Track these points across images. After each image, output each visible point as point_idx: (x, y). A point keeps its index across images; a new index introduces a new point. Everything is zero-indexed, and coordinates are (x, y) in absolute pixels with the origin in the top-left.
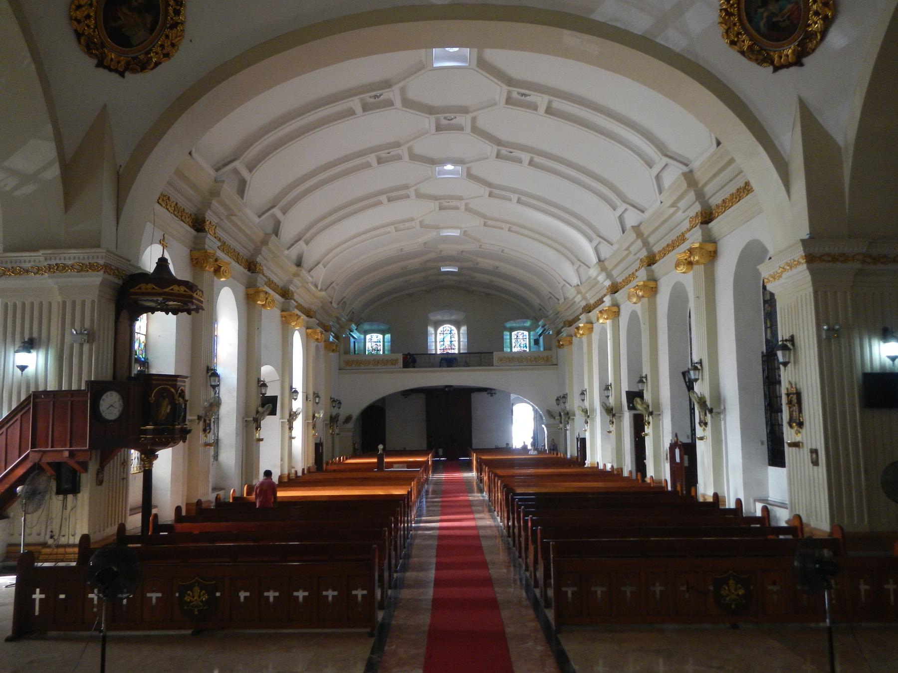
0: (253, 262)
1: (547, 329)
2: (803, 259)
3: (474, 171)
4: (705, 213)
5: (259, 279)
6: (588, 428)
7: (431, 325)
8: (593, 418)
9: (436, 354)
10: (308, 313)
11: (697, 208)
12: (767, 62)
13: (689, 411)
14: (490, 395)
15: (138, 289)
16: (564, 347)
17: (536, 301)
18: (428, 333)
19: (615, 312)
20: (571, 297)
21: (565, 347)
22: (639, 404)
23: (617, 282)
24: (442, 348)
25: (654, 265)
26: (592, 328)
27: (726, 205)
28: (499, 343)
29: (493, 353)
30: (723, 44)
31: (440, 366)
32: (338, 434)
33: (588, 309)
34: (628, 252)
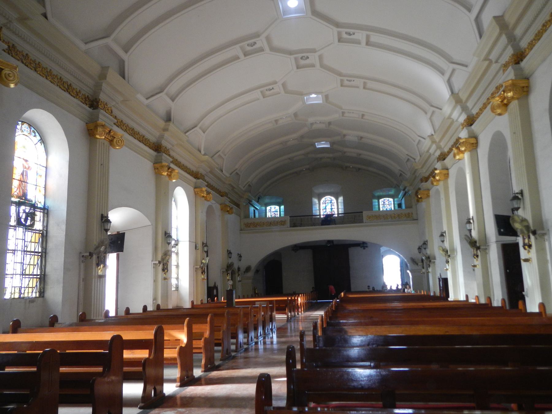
0: (96, 99)
1: (407, 192)
3: (320, 7)
5: (101, 116)
6: (449, 267)
7: (315, 197)
8: (454, 257)
10: (196, 175)
14: (363, 248)
16: (422, 201)
17: (395, 168)
18: (313, 203)
20: (426, 149)
21: (424, 200)
22: (517, 222)
23: (473, 114)
24: (325, 214)
25: (525, 60)
26: (448, 174)
29: (362, 212)
32: (240, 281)
34: (487, 63)
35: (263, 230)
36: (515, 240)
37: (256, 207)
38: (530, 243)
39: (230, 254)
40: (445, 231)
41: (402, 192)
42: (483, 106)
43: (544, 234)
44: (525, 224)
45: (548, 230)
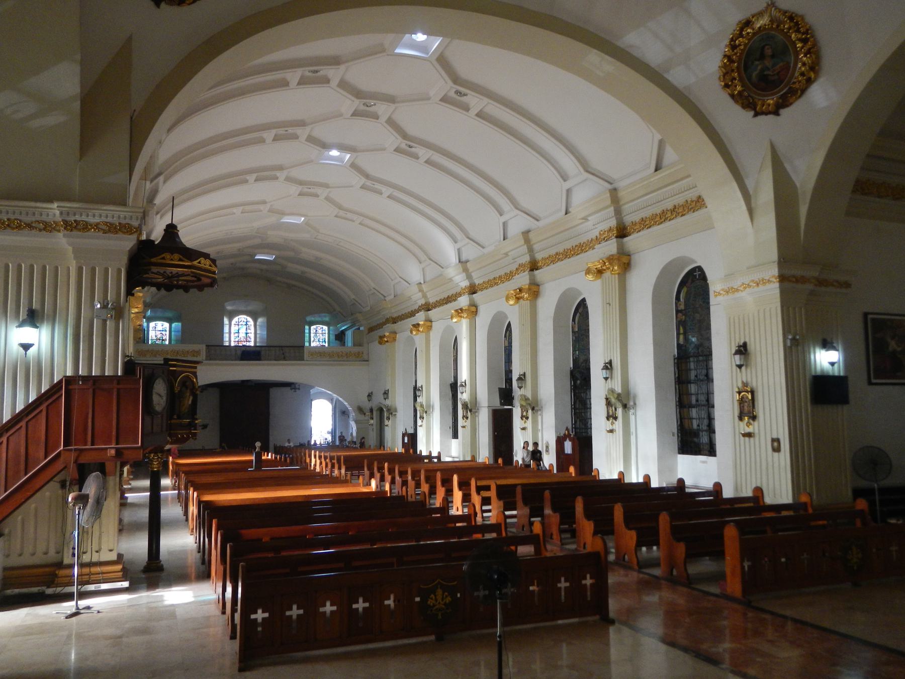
2: (776, 279)
4: (620, 228)
7: (227, 317)
8: (430, 414)
9: (230, 346)
11: (613, 223)
12: (751, 107)
13: (570, 407)
15: (161, 259)
16: (385, 344)
19: (473, 311)
24: (237, 340)
25: (537, 271)
26: (431, 326)
27: (645, 224)
30: (716, 85)
31: (242, 359)
33: (427, 307)
34: (504, 255)
42: (488, 282)
45: (542, 407)
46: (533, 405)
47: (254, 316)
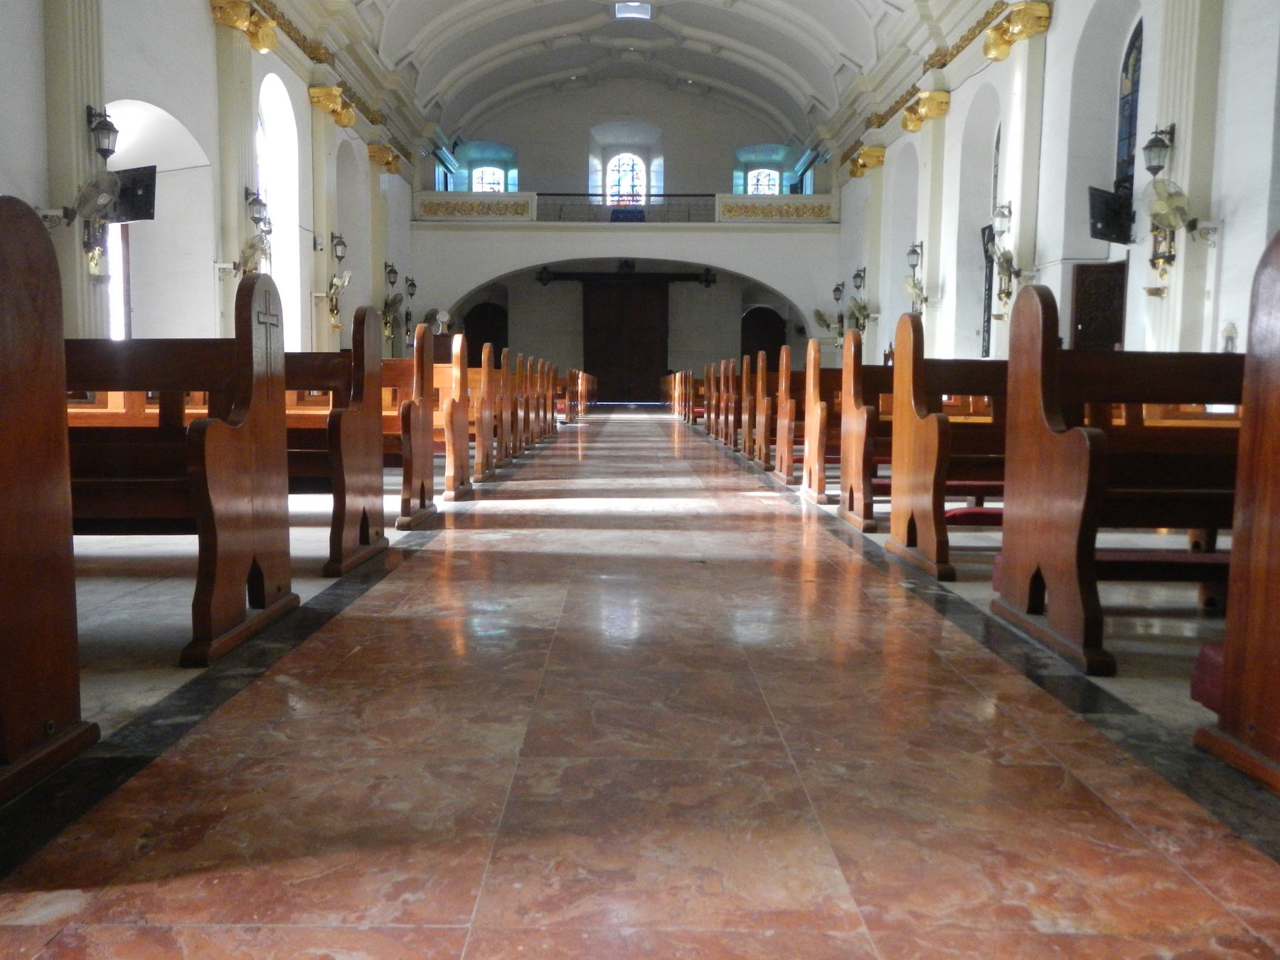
7: (596, 156)
8: (935, 303)
10: (315, 52)
14: (704, 284)
16: (862, 174)
17: (801, 89)
18: (591, 170)
21: (867, 172)
26: (947, 103)
28: (728, 186)
29: (714, 196)
35: (469, 223)
36: (1106, 257)
37: (449, 166)
38: (1173, 253)
39: (392, 275)
40: (922, 243)
41: (808, 152)
43: (1206, 233)
44: (1178, 202)
45: (1223, 221)
46: (1190, 217)
47: (646, 154)
